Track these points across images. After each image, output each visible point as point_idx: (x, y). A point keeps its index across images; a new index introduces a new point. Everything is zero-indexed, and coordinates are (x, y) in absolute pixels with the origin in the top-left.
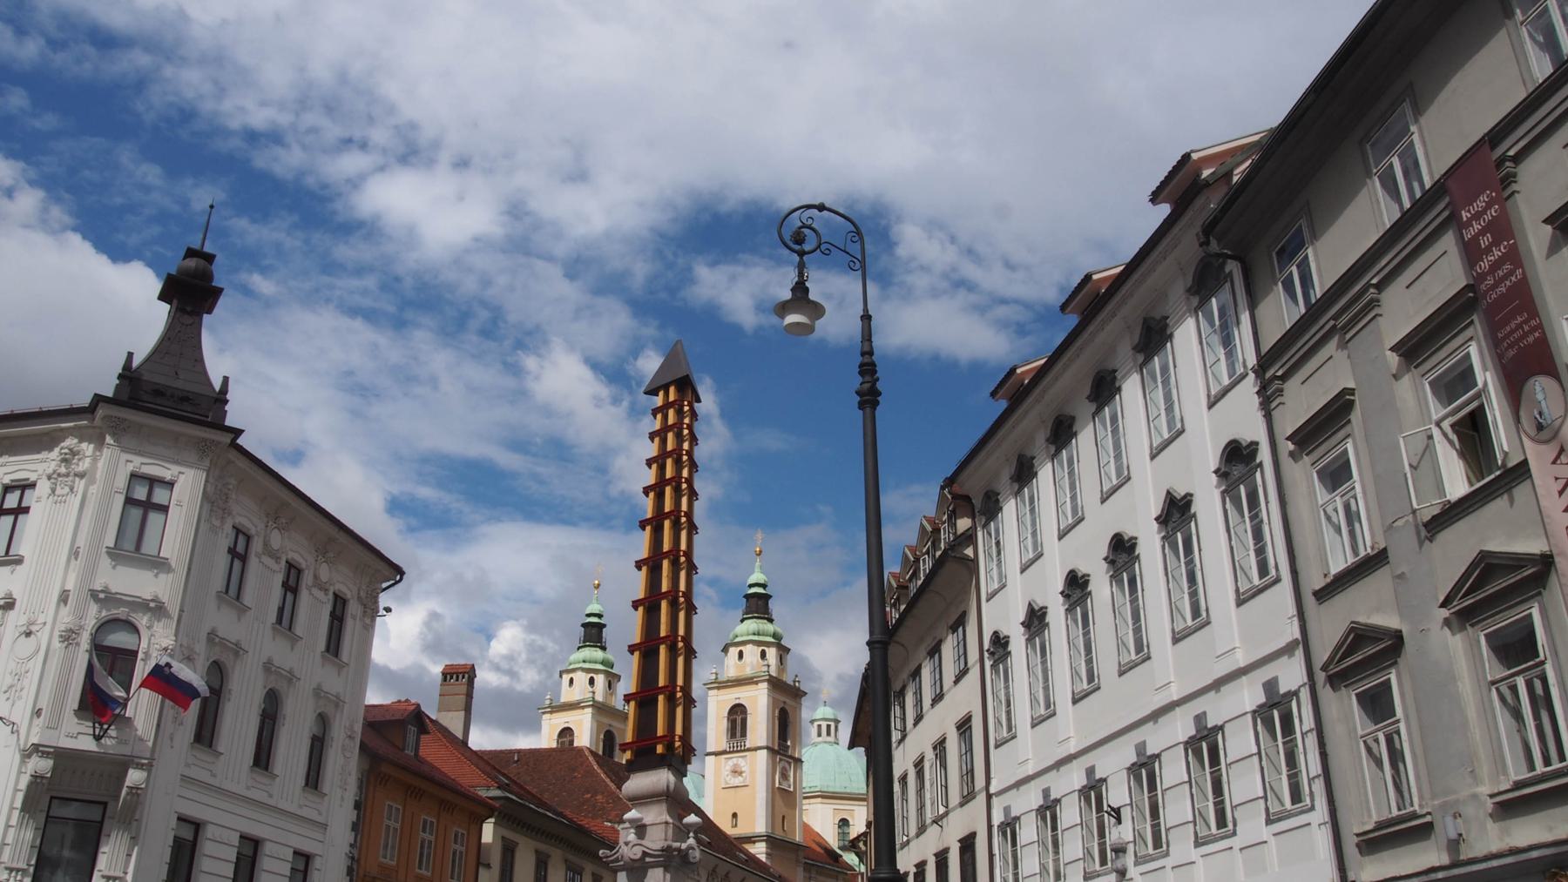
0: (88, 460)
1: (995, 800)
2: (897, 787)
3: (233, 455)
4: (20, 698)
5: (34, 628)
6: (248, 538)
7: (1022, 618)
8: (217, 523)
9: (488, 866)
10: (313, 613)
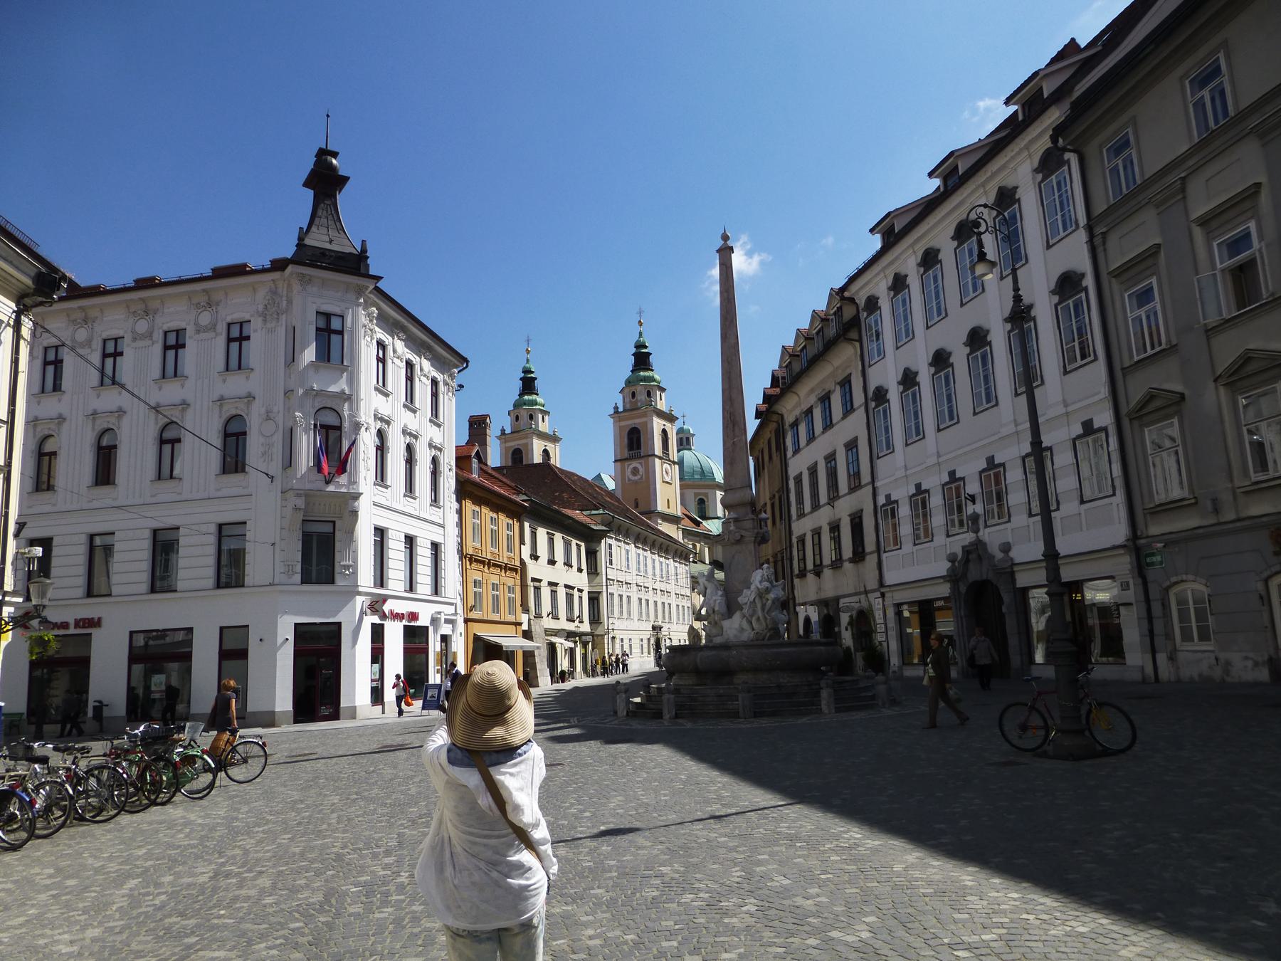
2: (792, 484)
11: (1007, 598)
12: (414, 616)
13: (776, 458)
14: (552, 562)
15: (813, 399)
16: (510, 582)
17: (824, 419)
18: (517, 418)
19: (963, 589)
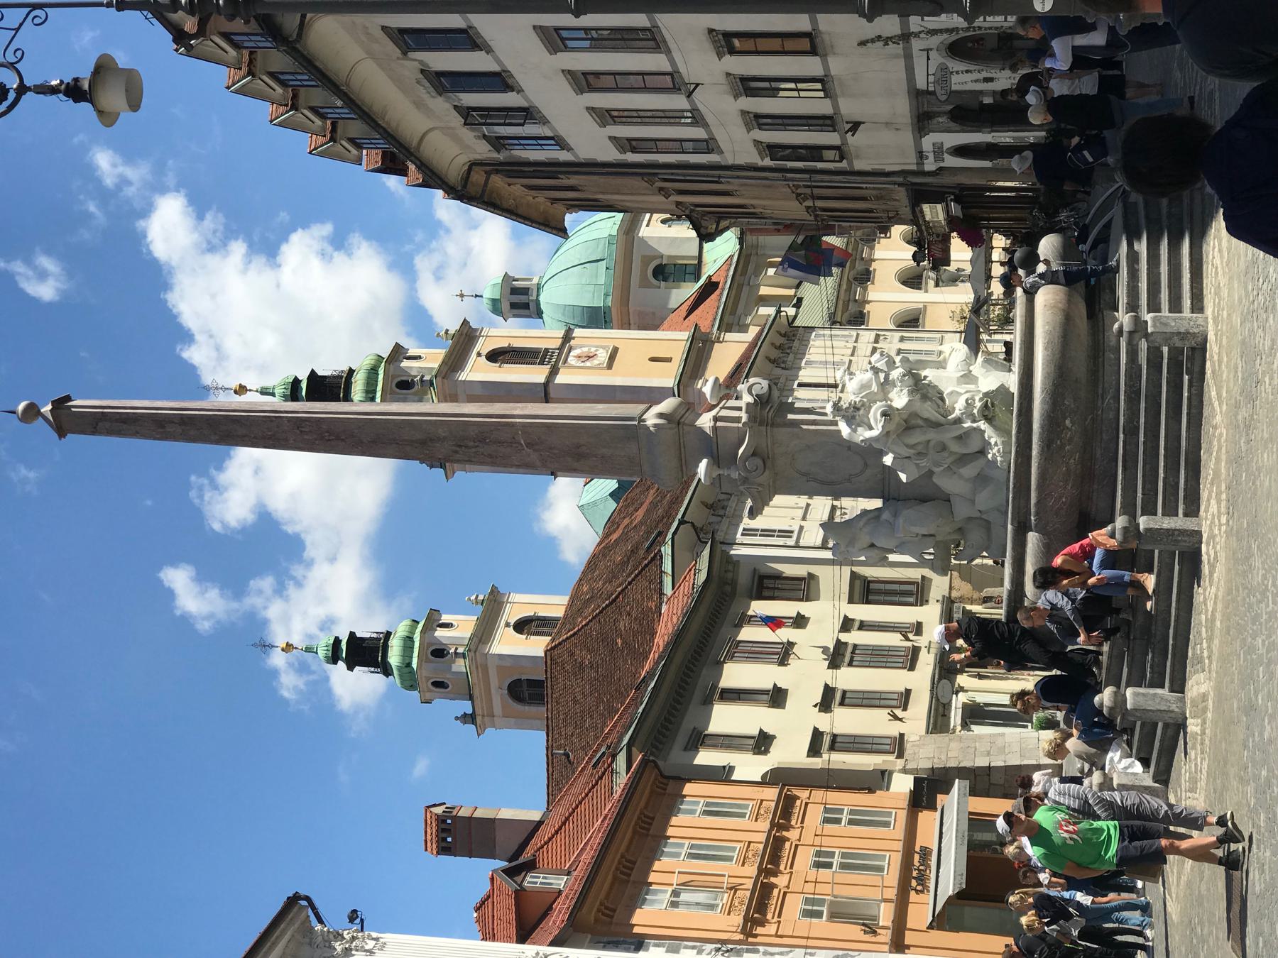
15: (441, 105)
16: (815, 815)
18: (438, 684)
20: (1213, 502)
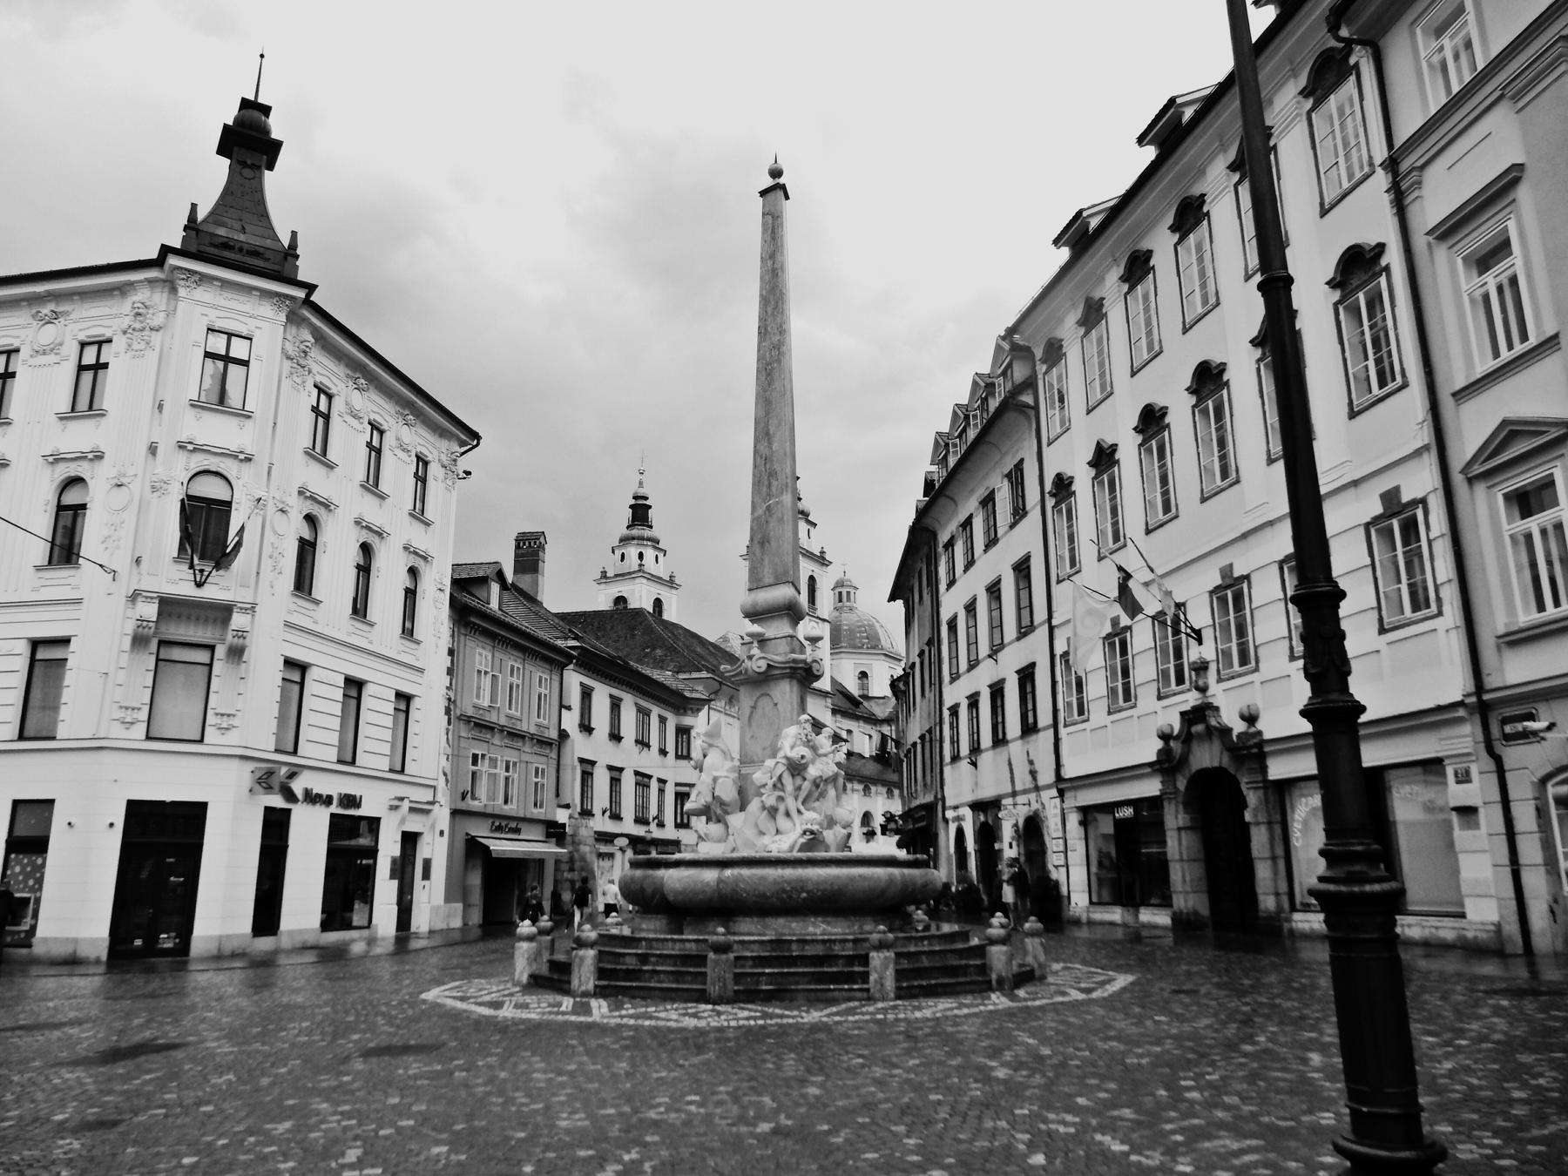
0: (162, 315)
1: (1057, 632)
3: (306, 313)
4: (118, 547)
5: (124, 480)
6: (330, 397)
7: (1089, 456)
8: (299, 380)
9: (569, 708)
10: (397, 474)
11: (1252, 798)
12: (350, 801)
13: (927, 598)
14: (616, 737)
17: (987, 532)
19: (1181, 784)
20: (746, 1014)
